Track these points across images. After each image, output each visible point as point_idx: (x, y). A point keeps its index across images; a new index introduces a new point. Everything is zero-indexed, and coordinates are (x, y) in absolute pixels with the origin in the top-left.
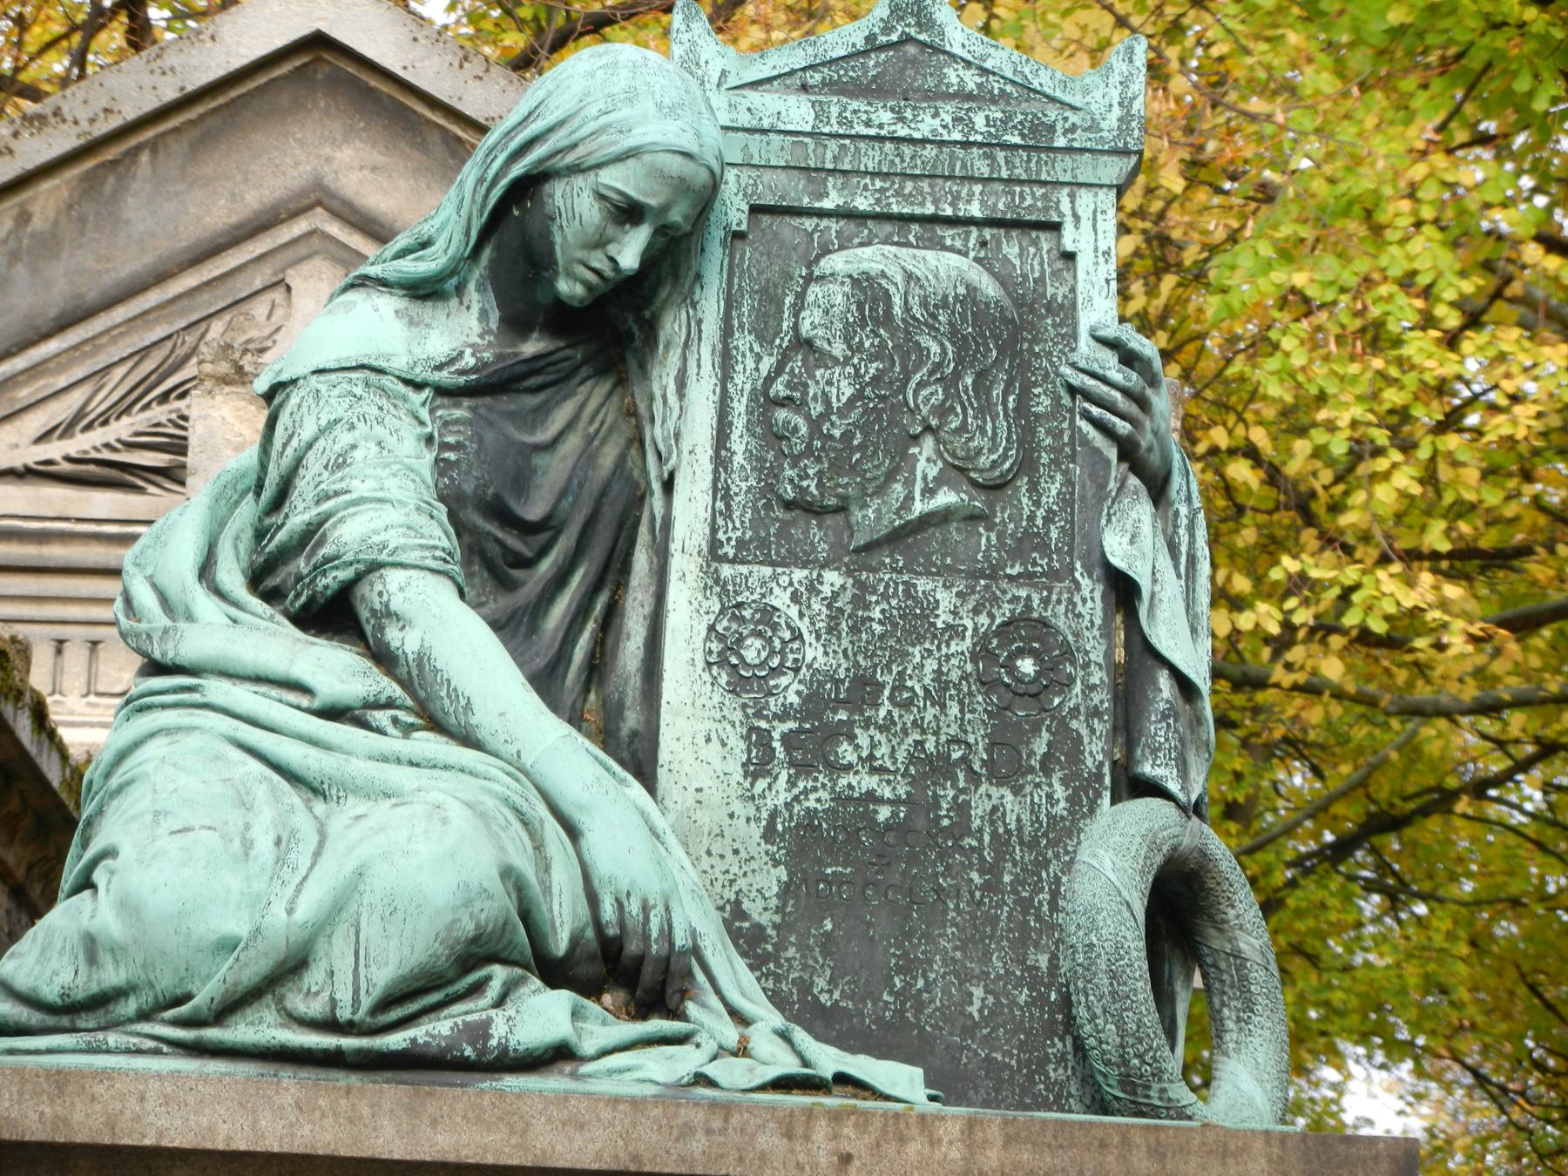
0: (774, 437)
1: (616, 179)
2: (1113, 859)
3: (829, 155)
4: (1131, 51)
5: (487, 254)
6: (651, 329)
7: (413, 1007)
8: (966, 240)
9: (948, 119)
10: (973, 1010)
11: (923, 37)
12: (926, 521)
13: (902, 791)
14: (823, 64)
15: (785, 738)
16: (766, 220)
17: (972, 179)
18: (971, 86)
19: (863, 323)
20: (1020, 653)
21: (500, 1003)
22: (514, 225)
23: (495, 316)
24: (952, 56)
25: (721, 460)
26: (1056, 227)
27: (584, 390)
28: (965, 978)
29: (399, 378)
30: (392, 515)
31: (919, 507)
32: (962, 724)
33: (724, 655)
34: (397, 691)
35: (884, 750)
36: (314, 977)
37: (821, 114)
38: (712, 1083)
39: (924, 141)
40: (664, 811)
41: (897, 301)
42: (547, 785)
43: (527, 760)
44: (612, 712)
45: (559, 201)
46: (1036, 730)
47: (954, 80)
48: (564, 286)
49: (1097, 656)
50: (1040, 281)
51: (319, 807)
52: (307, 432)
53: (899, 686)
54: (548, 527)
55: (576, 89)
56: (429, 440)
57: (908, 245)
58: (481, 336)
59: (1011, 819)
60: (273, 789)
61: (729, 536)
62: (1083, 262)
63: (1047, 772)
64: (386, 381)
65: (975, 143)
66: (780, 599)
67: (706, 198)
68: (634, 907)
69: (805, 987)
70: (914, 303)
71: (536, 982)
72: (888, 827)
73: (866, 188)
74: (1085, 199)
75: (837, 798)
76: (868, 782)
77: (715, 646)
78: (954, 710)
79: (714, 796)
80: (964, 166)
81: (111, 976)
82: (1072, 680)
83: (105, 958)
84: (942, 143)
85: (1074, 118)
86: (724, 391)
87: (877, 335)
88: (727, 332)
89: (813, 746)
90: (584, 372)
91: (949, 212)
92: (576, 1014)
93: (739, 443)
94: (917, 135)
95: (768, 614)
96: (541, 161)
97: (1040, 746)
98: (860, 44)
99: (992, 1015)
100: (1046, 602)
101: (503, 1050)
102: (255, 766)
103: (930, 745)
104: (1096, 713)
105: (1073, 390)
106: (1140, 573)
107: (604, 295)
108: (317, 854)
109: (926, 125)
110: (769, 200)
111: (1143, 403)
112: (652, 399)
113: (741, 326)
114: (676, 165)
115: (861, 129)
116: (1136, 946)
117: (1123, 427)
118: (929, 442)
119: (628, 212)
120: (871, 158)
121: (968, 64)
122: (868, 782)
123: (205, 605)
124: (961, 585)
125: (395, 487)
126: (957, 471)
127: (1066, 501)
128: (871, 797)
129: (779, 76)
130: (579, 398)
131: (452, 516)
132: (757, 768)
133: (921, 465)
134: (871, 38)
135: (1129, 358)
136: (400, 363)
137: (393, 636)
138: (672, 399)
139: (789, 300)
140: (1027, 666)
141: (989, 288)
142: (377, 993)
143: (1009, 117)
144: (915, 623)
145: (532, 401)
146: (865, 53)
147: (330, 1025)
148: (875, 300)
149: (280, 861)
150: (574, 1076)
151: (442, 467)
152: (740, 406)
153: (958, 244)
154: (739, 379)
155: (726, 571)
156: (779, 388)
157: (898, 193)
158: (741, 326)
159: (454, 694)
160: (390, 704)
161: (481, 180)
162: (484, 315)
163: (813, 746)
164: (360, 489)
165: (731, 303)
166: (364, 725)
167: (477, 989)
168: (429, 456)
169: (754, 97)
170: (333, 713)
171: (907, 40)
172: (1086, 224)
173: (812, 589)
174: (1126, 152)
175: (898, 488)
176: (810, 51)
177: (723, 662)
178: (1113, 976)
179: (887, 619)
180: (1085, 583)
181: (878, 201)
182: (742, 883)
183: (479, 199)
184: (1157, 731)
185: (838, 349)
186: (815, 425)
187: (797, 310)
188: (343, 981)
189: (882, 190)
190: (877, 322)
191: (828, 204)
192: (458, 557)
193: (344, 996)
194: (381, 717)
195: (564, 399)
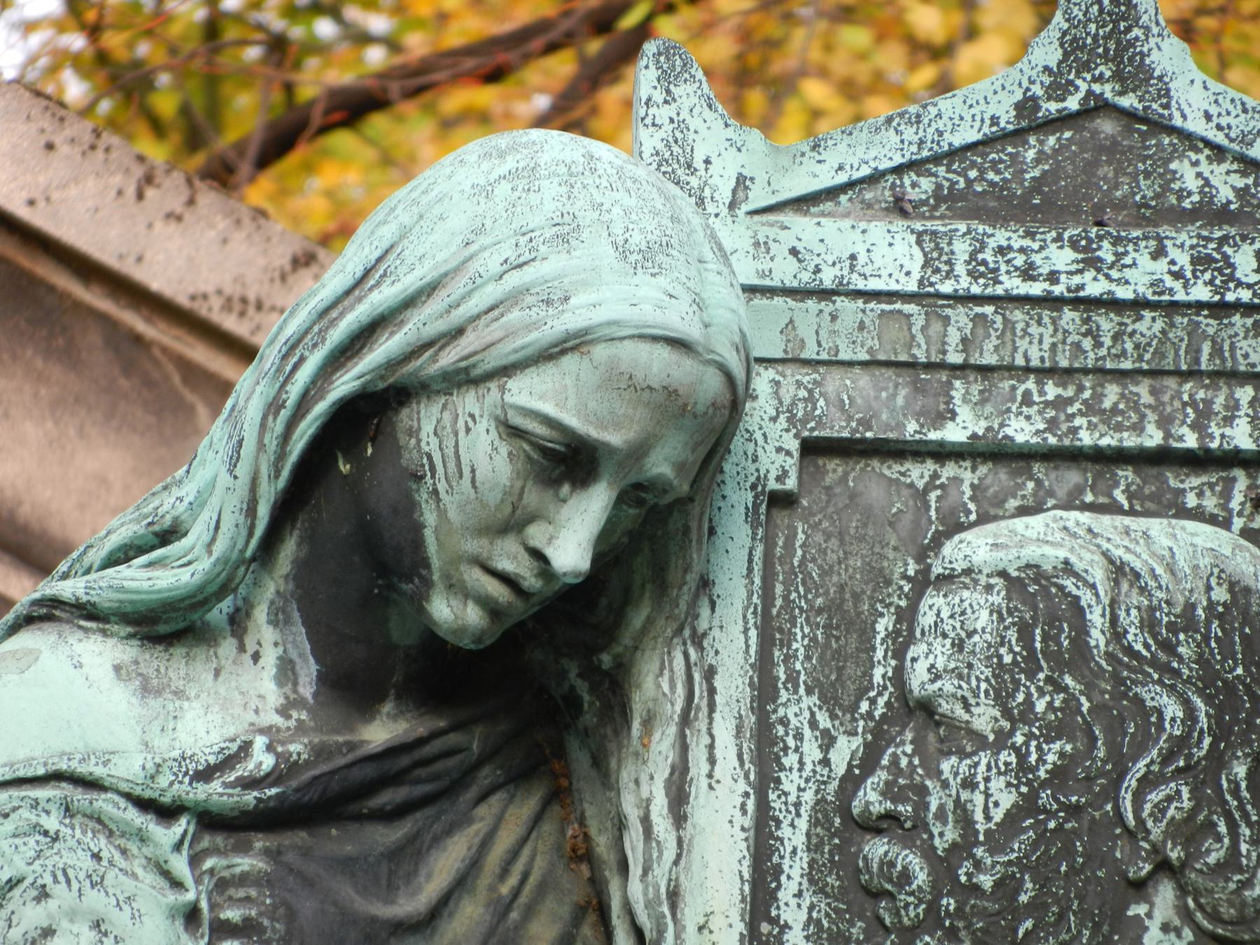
3: (954, 337)
5: (289, 550)
6: (614, 691)
8: (1226, 495)
9: (1183, 259)
11: (1128, 101)
14: (936, 159)
16: (834, 468)
18: (1225, 194)
19: (1031, 666)
22: (342, 486)
23: (308, 671)
24: (1189, 139)
27: (486, 812)
29: (128, 796)
37: (935, 257)
39: (1138, 305)
41: (1096, 618)
45: (429, 443)
47: (1192, 184)
48: (444, 610)
55: (458, 221)
57: (1112, 508)
58: (283, 712)
65: (1237, 306)
67: (716, 429)
73: (1027, 400)
80: (1217, 351)
86: (763, 806)
87: (1059, 688)
88: (764, 692)
90: (486, 776)
91: (1191, 441)
94: (1124, 293)
96: (393, 364)
98: (1007, 118)
107: (521, 625)
109: (1141, 274)
110: (840, 429)
112: (621, 825)
113: (792, 678)
114: (658, 364)
115: (1013, 284)
118: (1165, 894)
119: (566, 461)
121: (1219, 153)
129: (850, 185)
130: (477, 829)
134: (1027, 106)
136: (128, 768)
139: (884, 625)
146: (1017, 136)
148: (1053, 620)
152: (794, 836)
153: (1210, 503)
156: (870, 797)
157: (1091, 408)
158: (792, 678)
161: (274, 407)
162: (286, 672)
165: (770, 636)
169: (802, 227)
171: (1096, 107)
176: (909, 133)
181: (1052, 425)
183: (271, 442)
185: (984, 718)
187: (901, 643)
189: (1060, 403)
190: (1059, 663)
191: (954, 433)
195: (449, 832)
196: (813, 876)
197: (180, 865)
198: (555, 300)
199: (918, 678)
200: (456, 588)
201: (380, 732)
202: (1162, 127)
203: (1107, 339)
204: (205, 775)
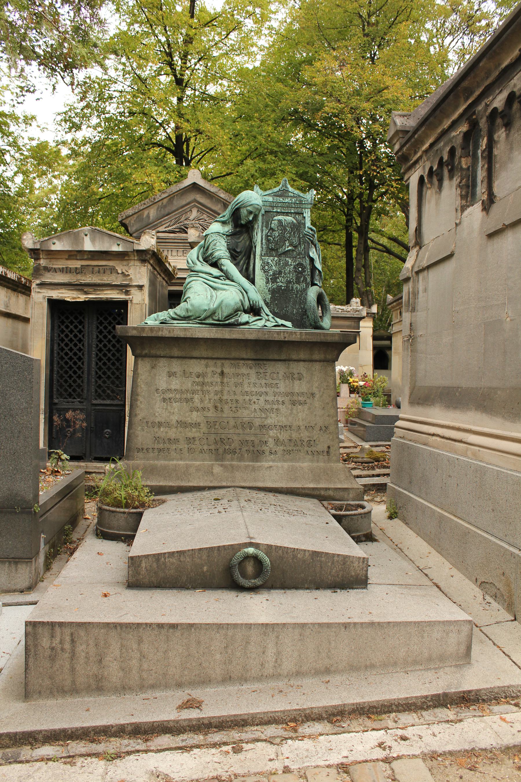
0: (268, 241)
1: (249, 208)
12: (287, 251)
22: (236, 214)
25: (262, 244)
26: (303, 214)
28: (293, 308)
32: (292, 277)
33: (263, 268)
36: (216, 314)
61: (263, 253)
66: (270, 261)
69: (274, 310)
74: (306, 210)
79: (262, 286)
81: (190, 314)
89: (274, 280)
93: (264, 241)
95: (268, 263)
99: (297, 313)
109: (287, 201)
116: (316, 305)
119: (250, 213)
123: (198, 263)
126: (291, 245)
127: (304, 248)
132: (267, 283)
135: (312, 230)
136: (222, 232)
137: (223, 267)
140: (300, 269)
141: (295, 221)
144: (287, 264)
147: (218, 320)
151: (227, 245)
152: (264, 237)
163: (274, 280)
164: (218, 248)
165: (263, 223)
167: (237, 315)
184: (317, 277)
188: (220, 315)
193: (220, 317)
194: (222, 278)
201: (238, 230)
203: (284, 205)
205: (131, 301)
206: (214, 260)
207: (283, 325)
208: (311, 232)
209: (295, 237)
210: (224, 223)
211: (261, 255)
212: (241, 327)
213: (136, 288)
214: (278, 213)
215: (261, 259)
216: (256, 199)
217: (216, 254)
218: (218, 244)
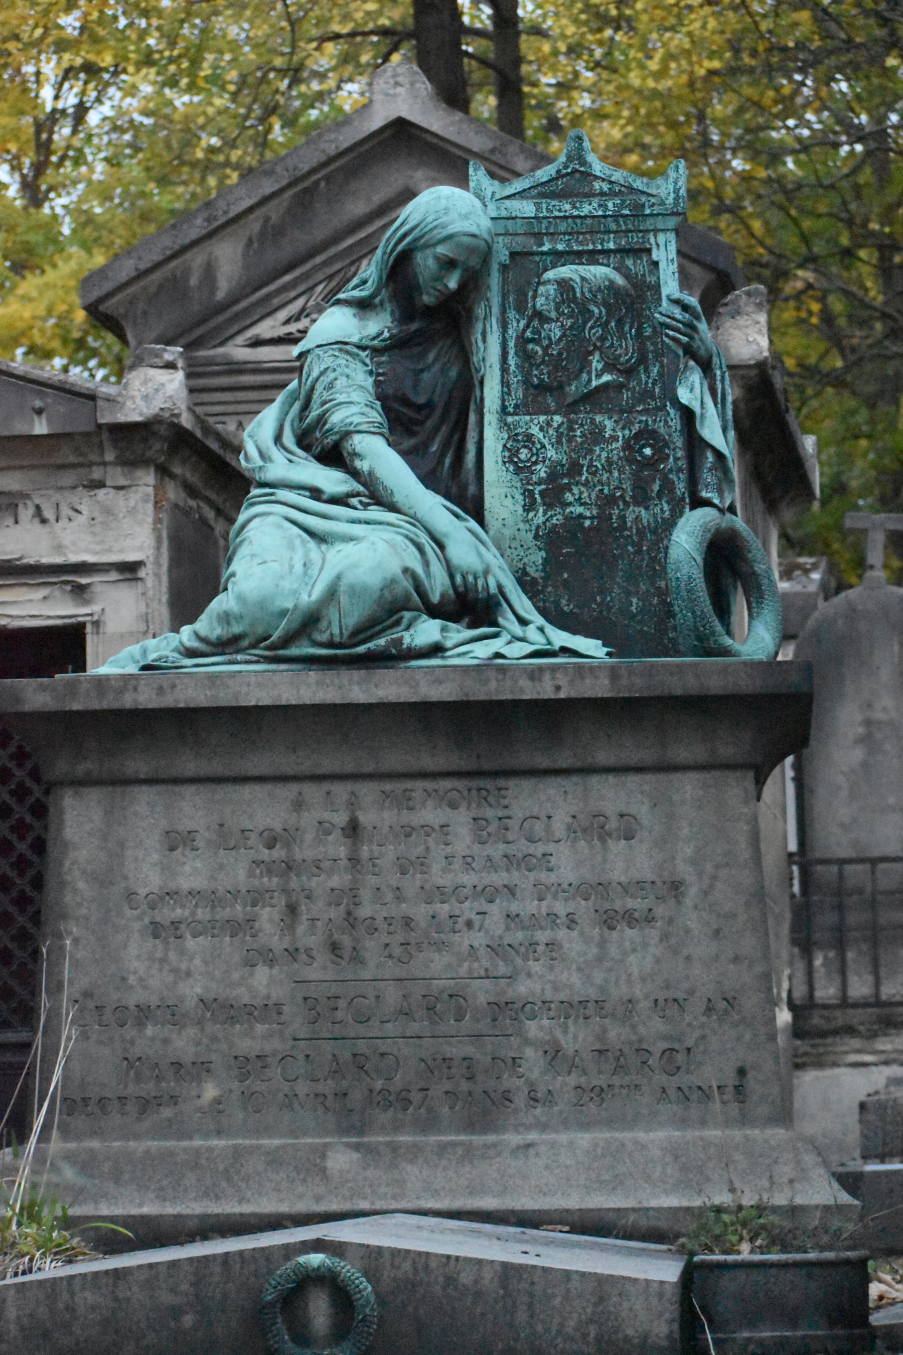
0: (526, 356)
1: (441, 250)
2: (687, 538)
4: (677, 167)
6: (469, 312)
7: (369, 633)
10: (633, 609)
12: (597, 388)
13: (595, 512)
15: (541, 493)
17: (609, 232)
18: (605, 189)
19: (563, 301)
20: (644, 446)
21: (407, 628)
23: (397, 314)
24: (597, 178)
25: (504, 370)
26: (649, 251)
27: (440, 344)
28: (628, 594)
30: (354, 409)
31: (594, 383)
32: (620, 480)
33: (511, 457)
34: (361, 488)
35: (585, 495)
36: (323, 624)
37: (538, 206)
38: (502, 656)
39: (586, 217)
40: (487, 532)
42: (429, 526)
43: (419, 515)
44: (464, 487)
46: (654, 480)
48: (426, 299)
49: (679, 444)
50: (643, 275)
51: (324, 547)
52: (315, 374)
53: (590, 466)
54: (429, 405)
56: (371, 373)
59: (645, 521)
60: (304, 542)
61: (511, 403)
62: (662, 266)
63: (660, 499)
64: (348, 347)
66: (535, 430)
67: (486, 255)
68: (470, 578)
69: (557, 603)
70: (586, 290)
71: (425, 617)
72: (590, 528)
74: (661, 238)
75: (566, 518)
76: (580, 510)
77: (507, 454)
78: (616, 474)
79: (510, 521)
81: (236, 629)
82: (668, 456)
83: (233, 622)
84: (594, 217)
85: (653, 200)
88: (503, 311)
89: (553, 495)
92: (443, 629)
93: (512, 361)
95: (529, 437)
96: (409, 244)
97: (656, 487)
99: (641, 611)
100: (655, 421)
101: (409, 649)
102: (296, 530)
103: (606, 491)
104: (680, 470)
105: (662, 325)
106: (696, 407)
108: (321, 570)
109: (586, 209)
110: (519, 249)
111: (694, 328)
115: (557, 214)
117: (685, 339)
118: (597, 356)
119: (449, 264)
120: (563, 227)
122: (580, 510)
123: (277, 454)
124: (615, 417)
125: (356, 396)
126: (609, 367)
127: (661, 374)
128: (581, 516)
131: (383, 406)
132: (529, 507)
133: (594, 364)
134: (558, 171)
135: (685, 308)
136: (355, 339)
137: (358, 464)
138: (480, 344)
139: (530, 294)
140: (648, 451)
141: (620, 280)
142: (350, 629)
143: (623, 202)
144: (596, 436)
145: (417, 350)
146: (557, 179)
147: (331, 645)
149: (305, 574)
150: (443, 658)
151: (377, 384)
152: (511, 344)
154: (510, 332)
155: (510, 419)
156: (528, 334)
157: (577, 241)
159: (385, 488)
160: (358, 494)
162: (392, 313)
163: (553, 495)
164: (341, 398)
165: (504, 296)
166: (348, 505)
167: (398, 623)
168: (371, 380)
169: (508, 203)
170: (336, 500)
171: (575, 171)
172: (662, 248)
173: (549, 424)
174: (677, 214)
175: (585, 376)
177: (511, 461)
178: (689, 591)
179: (583, 435)
180: (672, 411)
182: (525, 560)
184: (707, 477)
185: (553, 315)
186: (545, 349)
187: (534, 297)
188: (336, 625)
191: (545, 248)
192: (386, 425)
193: (336, 631)
194: (354, 501)
196: (516, 354)
197: (368, 361)
198: (444, 226)
199: (538, 305)
200: (428, 294)
201: (414, 326)
202: (590, 174)
203: (579, 225)
204: (374, 339)
205: (97, 624)
206: (330, 440)
207: (565, 651)
208: (677, 312)
209: (622, 336)
210: (363, 306)
211: (504, 410)
212: (414, 663)
213: (114, 576)
214: (560, 258)
215: (504, 425)
216: (466, 217)
217: (336, 418)
218: (341, 382)
